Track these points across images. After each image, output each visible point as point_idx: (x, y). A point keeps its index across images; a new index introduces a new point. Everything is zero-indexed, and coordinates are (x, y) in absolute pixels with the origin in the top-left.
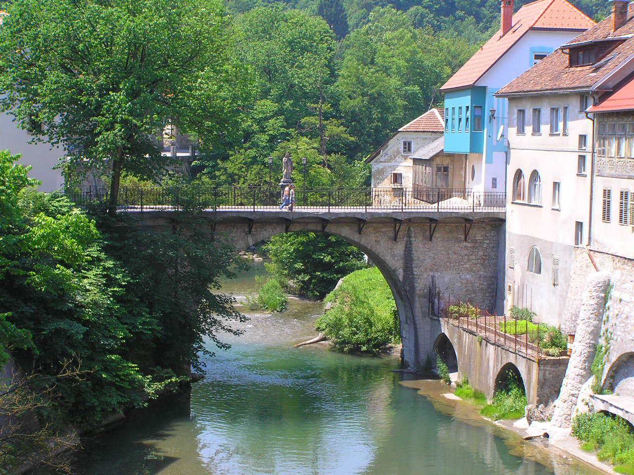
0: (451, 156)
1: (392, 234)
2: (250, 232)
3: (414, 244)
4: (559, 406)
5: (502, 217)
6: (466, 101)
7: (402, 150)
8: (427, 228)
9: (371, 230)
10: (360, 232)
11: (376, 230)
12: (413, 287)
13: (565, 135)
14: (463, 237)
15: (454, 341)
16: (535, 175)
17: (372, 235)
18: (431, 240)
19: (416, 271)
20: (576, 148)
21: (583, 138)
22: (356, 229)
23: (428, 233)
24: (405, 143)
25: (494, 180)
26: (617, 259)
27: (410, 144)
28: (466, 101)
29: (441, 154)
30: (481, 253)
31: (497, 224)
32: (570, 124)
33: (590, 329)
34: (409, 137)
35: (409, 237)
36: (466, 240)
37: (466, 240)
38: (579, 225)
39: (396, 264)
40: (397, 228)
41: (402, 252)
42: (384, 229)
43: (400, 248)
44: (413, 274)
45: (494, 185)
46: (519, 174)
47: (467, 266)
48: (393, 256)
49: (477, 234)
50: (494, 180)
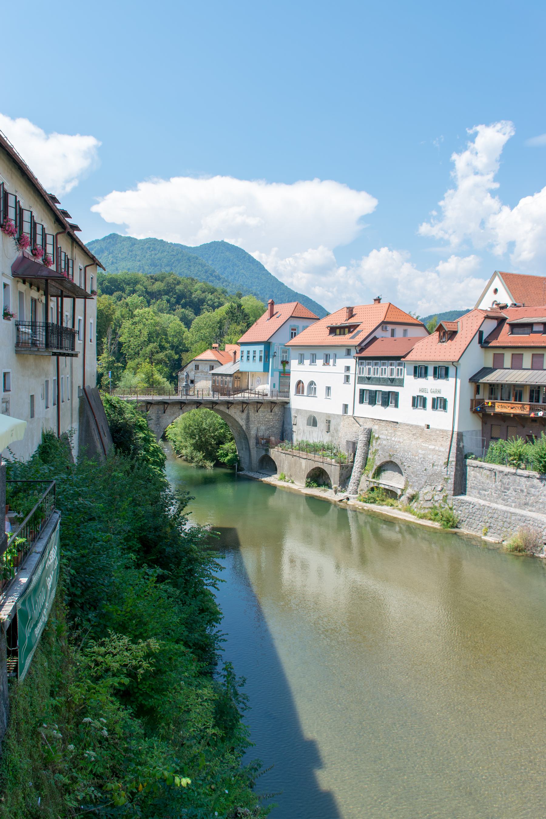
0: (241, 373)
1: (241, 409)
2: (181, 409)
3: (251, 414)
4: (351, 486)
5: (288, 401)
6: (262, 347)
7: (194, 369)
13: (334, 365)
16: (312, 383)
19: (251, 426)
20: (343, 372)
21: (348, 368)
24: (196, 366)
25: (274, 384)
26: (375, 421)
27: (198, 366)
28: (262, 347)
29: (238, 372)
30: (277, 418)
31: (285, 405)
32: (337, 360)
33: (364, 451)
34: (198, 363)
35: (248, 410)
36: (271, 411)
38: (346, 406)
42: (238, 407)
43: (244, 415)
45: (274, 387)
46: (300, 382)
48: (242, 419)
49: (276, 409)
50: (274, 384)
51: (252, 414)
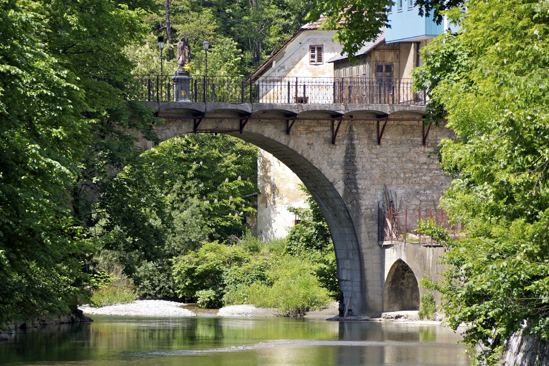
1: (329, 135)
3: (358, 148)
8: (374, 128)
9: (301, 128)
10: (287, 131)
11: (308, 130)
12: (358, 207)
14: (420, 139)
15: (414, 266)
17: (304, 136)
18: (379, 143)
19: (362, 184)
22: (283, 127)
23: (375, 135)
35: (351, 139)
36: (424, 143)
37: (424, 143)
39: (334, 174)
40: (335, 127)
41: (342, 159)
42: (319, 129)
43: (338, 153)
44: (357, 188)
47: (427, 178)
48: (331, 164)
51: (363, 149)
